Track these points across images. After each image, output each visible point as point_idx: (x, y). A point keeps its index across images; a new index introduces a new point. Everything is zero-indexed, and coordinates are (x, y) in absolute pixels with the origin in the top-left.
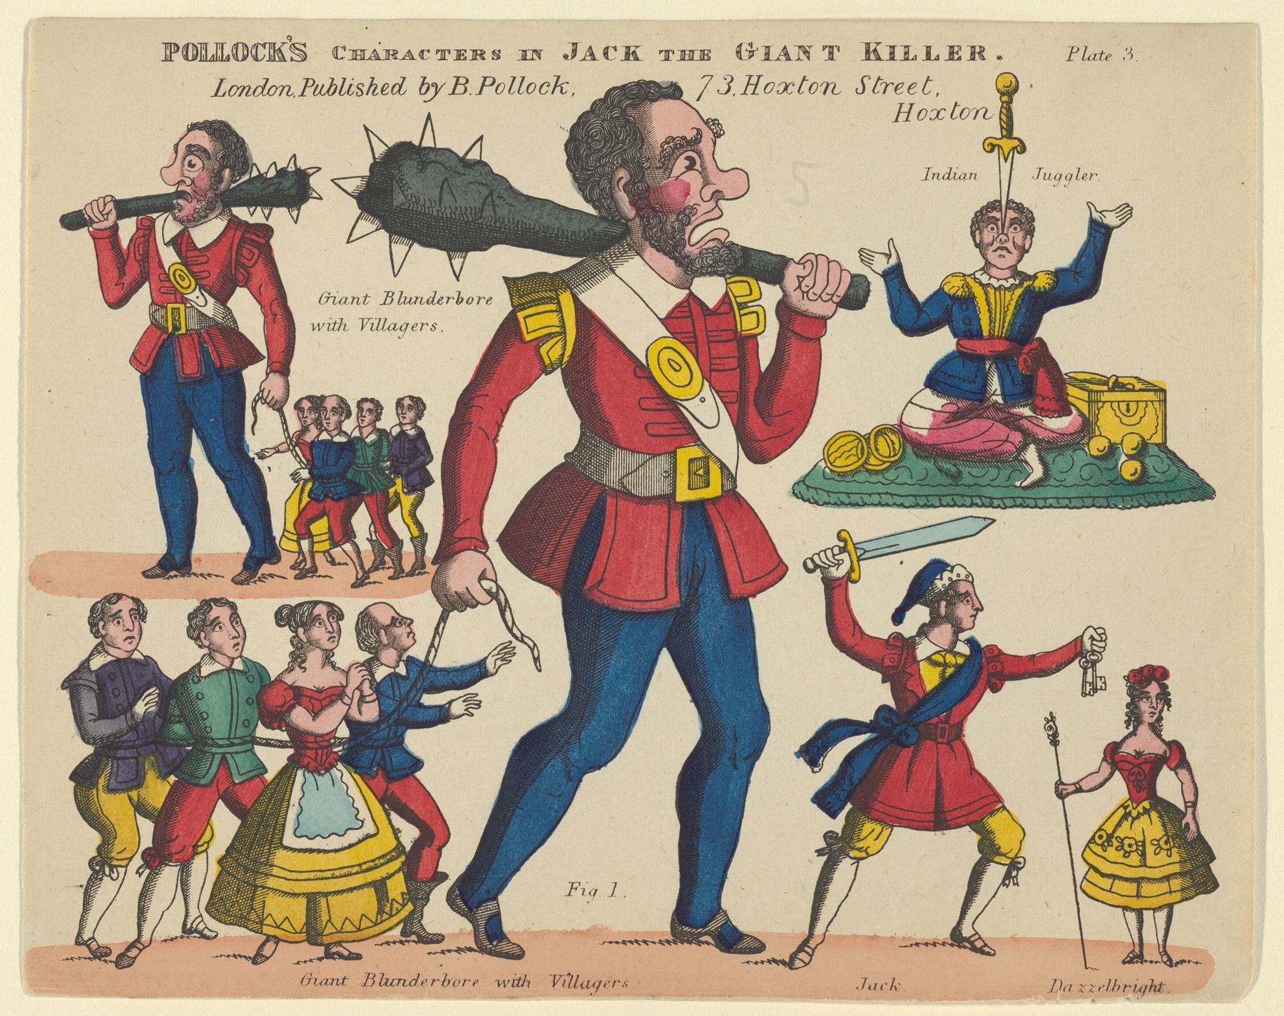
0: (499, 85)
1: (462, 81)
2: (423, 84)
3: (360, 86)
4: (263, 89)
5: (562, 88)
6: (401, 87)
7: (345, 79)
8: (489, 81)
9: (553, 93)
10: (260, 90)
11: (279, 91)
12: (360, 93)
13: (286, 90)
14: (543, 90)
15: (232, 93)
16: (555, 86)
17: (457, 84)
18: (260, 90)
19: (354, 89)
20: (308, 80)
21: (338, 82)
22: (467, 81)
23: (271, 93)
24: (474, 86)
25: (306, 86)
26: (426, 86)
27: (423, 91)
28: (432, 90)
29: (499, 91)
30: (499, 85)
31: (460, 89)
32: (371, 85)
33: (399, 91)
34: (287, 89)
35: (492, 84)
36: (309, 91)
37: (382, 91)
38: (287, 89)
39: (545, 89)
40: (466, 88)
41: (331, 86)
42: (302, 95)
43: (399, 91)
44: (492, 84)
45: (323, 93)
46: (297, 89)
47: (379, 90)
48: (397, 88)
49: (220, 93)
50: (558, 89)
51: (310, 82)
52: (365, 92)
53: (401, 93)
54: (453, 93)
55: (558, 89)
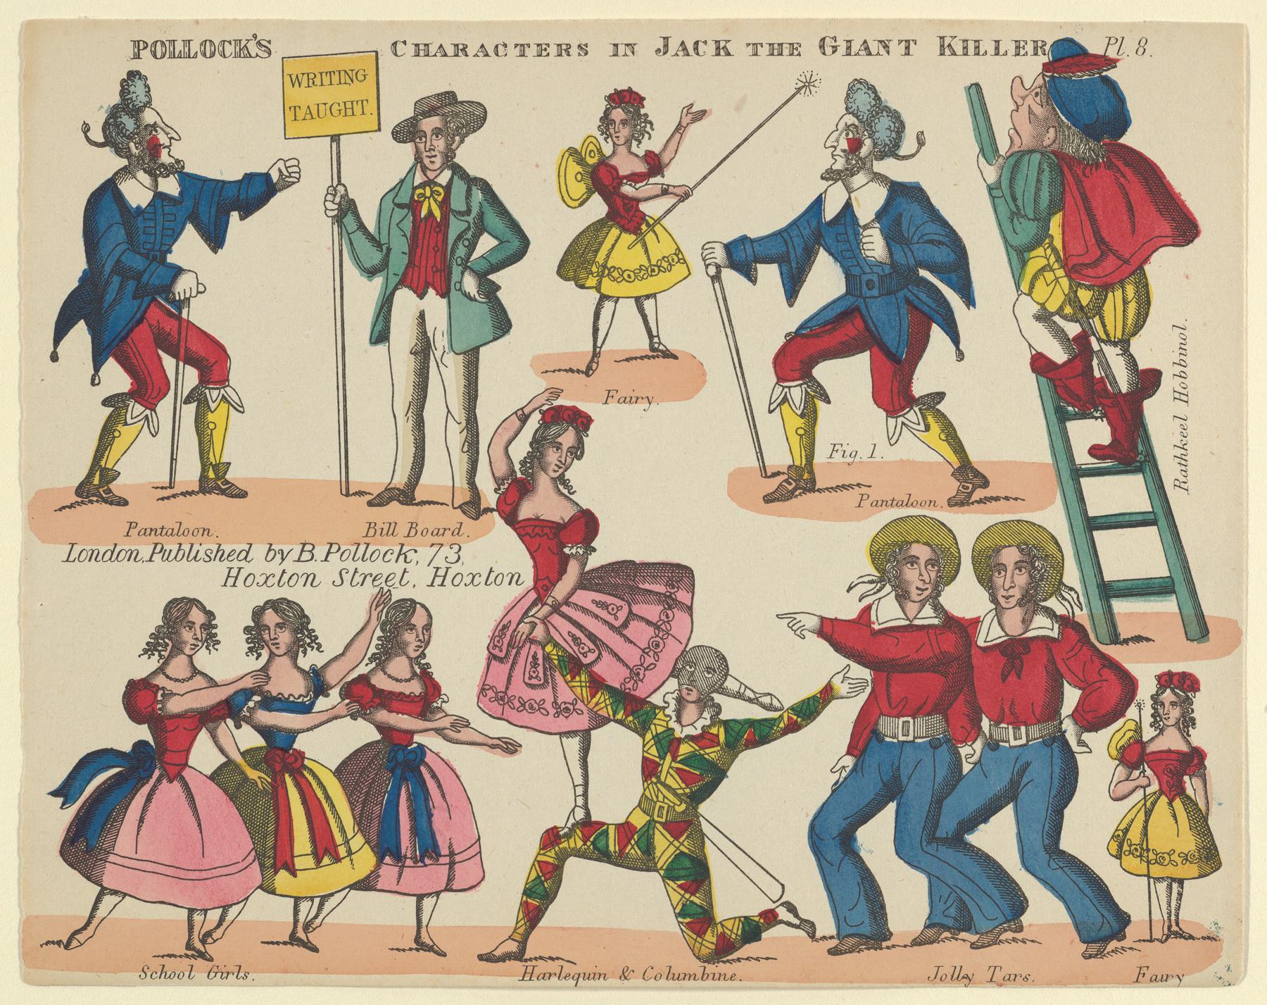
0: (343, 552)
2: (270, 550)
3: (208, 552)
5: (406, 557)
6: (248, 553)
9: (397, 561)
16: (400, 554)
17: (302, 551)
19: (201, 555)
27: (269, 559)
28: (279, 556)
30: (343, 552)
31: (306, 556)
32: (218, 551)
33: (246, 558)
35: (338, 551)
39: (388, 557)
40: (313, 555)
43: (246, 558)
44: (338, 551)
47: (226, 555)
48: (244, 554)
50: (402, 558)
52: (213, 556)
53: (248, 559)
55: (402, 558)
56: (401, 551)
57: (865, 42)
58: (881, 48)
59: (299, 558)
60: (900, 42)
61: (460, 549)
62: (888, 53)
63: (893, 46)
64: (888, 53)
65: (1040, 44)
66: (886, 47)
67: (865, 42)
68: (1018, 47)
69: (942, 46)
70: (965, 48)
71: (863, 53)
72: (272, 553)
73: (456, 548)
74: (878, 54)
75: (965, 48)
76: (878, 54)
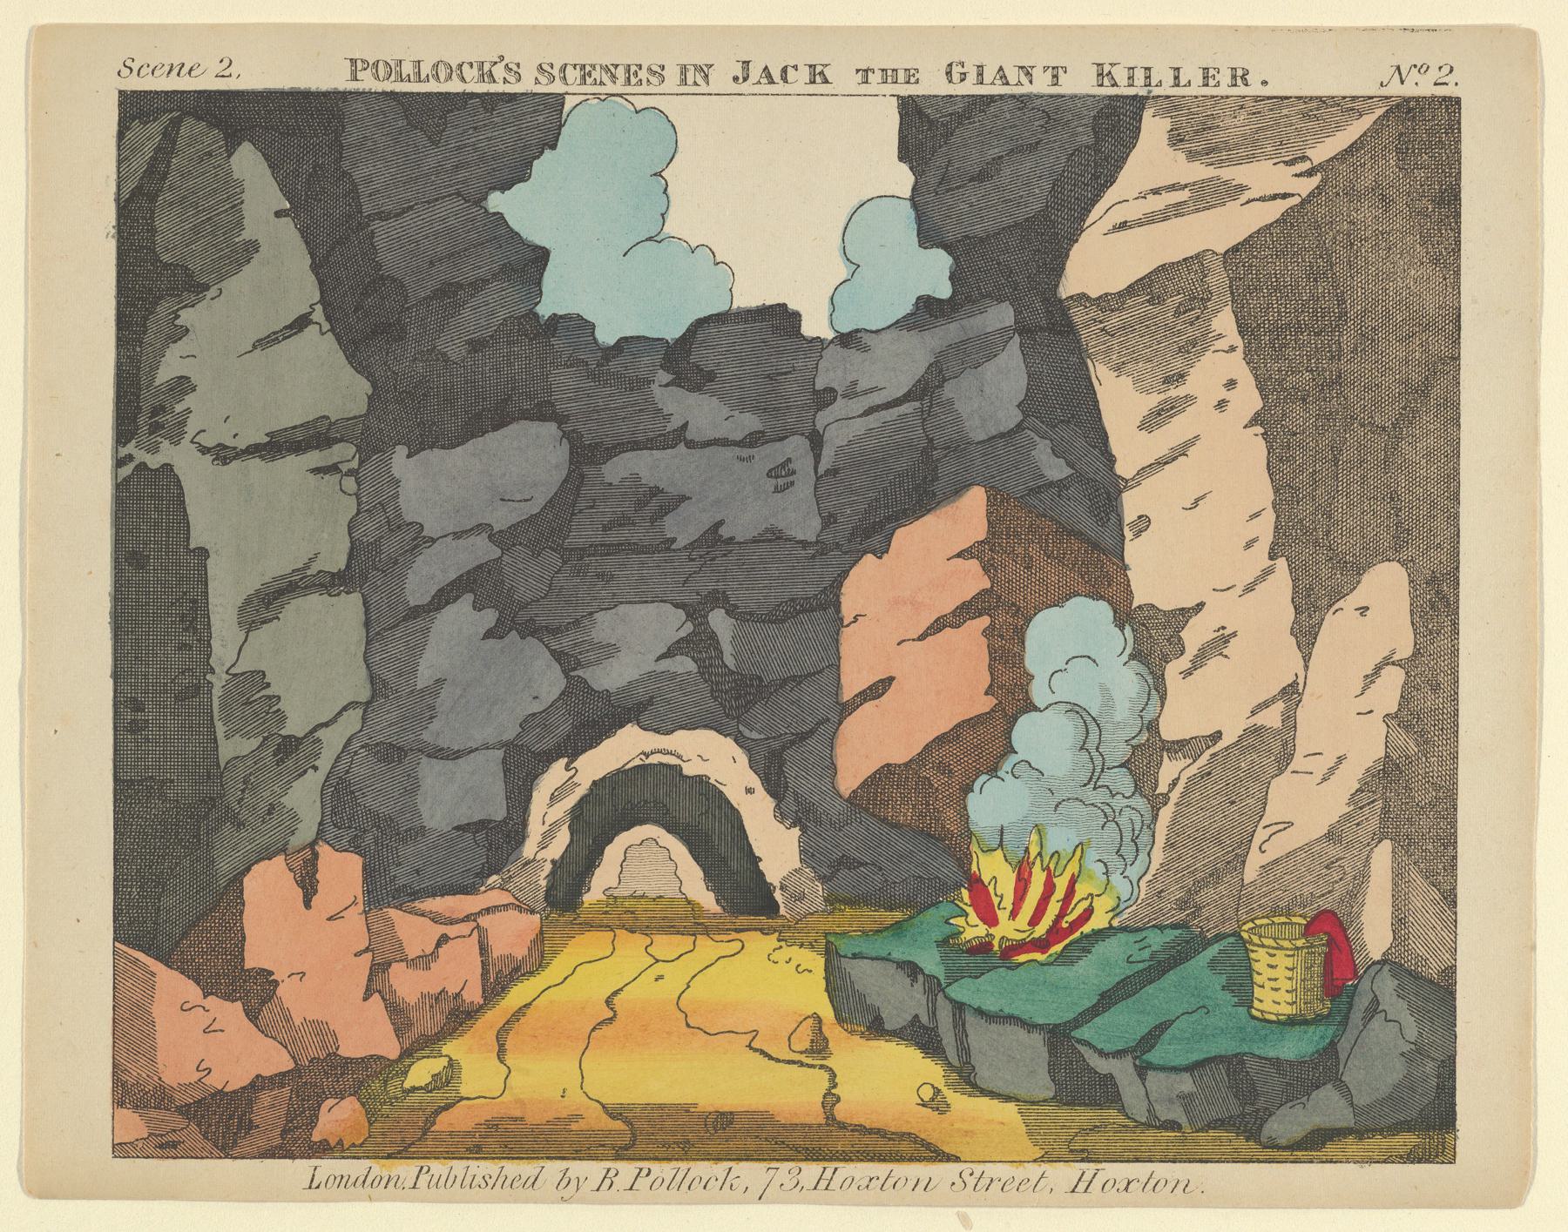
57: (1001, 69)
58: (1022, 75)
60: (1046, 69)
62: (1031, 82)
63: (1035, 73)
64: (1031, 82)
65: (1240, 73)
66: (1028, 74)
67: (1001, 69)
68: (1206, 77)
69: (1100, 75)
70: (1131, 78)
71: (1000, 82)
74: (1019, 83)
75: (1131, 78)
76: (1019, 83)
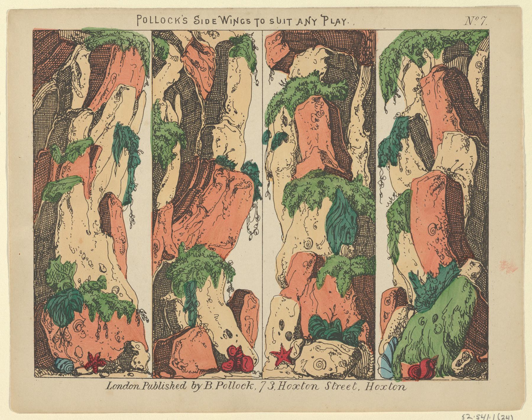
1: (209, 383)
2: (193, 384)
4: (127, 386)
6: (184, 385)
7: (161, 382)
8: (220, 383)
10: (126, 386)
11: (134, 387)
12: (167, 388)
13: (136, 387)
14: (243, 387)
15: (114, 388)
16: (248, 386)
17: (207, 385)
18: (126, 386)
19: (165, 386)
20: (146, 383)
21: (158, 384)
22: (212, 383)
23: (130, 388)
24: (214, 385)
25: (145, 386)
26: (194, 386)
27: (193, 387)
28: (197, 387)
29: (225, 388)
31: (209, 387)
33: (183, 387)
34: (137, 386)
35: (222, 385)
36: (146, 387)
37: (176, 387)
38: (137, 386)
40: (211, 387)
41: (155, 385)
42: (143, 389)
44: (222, 385)
45: (152, 388)
46: (141, 387)
49: (109, 388)
51: (147, 384)
52: (169, 387)
53: (184, 388)
54: (206, 388)
55: (249, 387)
56: (249, 384)
59: (206, 387)
61: (274, 384)
72: (194, 386)
73: (273, 383)
